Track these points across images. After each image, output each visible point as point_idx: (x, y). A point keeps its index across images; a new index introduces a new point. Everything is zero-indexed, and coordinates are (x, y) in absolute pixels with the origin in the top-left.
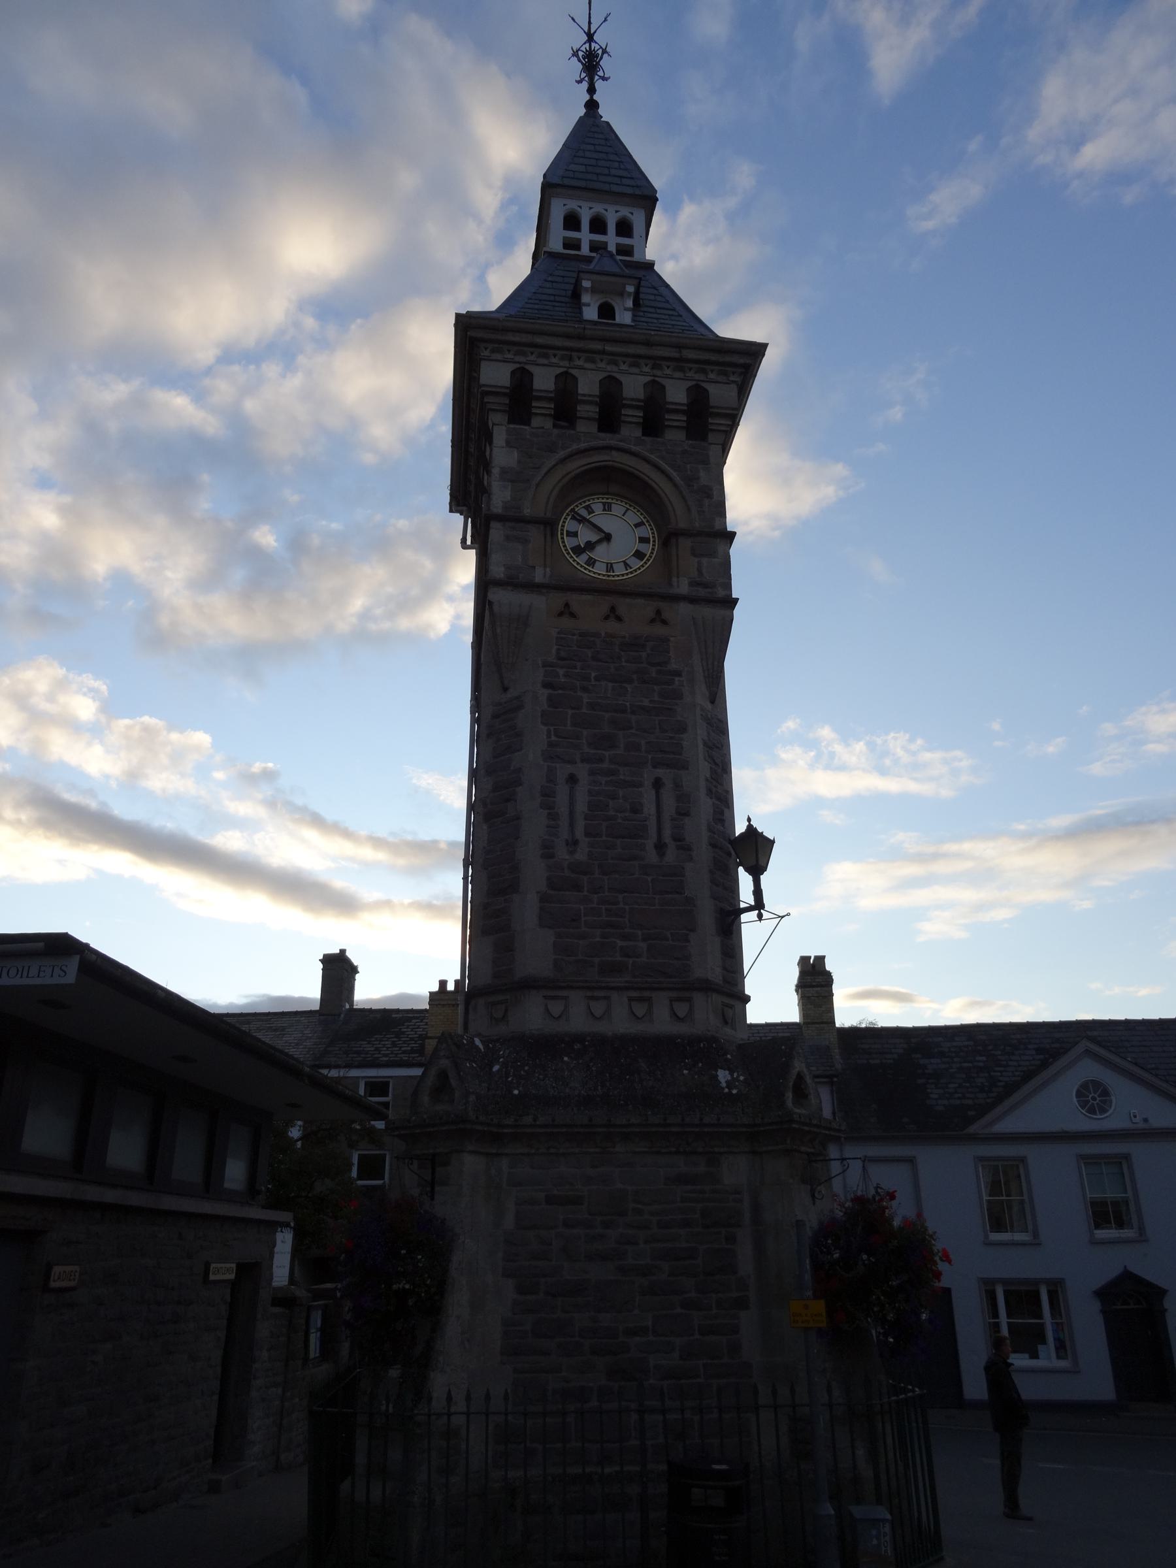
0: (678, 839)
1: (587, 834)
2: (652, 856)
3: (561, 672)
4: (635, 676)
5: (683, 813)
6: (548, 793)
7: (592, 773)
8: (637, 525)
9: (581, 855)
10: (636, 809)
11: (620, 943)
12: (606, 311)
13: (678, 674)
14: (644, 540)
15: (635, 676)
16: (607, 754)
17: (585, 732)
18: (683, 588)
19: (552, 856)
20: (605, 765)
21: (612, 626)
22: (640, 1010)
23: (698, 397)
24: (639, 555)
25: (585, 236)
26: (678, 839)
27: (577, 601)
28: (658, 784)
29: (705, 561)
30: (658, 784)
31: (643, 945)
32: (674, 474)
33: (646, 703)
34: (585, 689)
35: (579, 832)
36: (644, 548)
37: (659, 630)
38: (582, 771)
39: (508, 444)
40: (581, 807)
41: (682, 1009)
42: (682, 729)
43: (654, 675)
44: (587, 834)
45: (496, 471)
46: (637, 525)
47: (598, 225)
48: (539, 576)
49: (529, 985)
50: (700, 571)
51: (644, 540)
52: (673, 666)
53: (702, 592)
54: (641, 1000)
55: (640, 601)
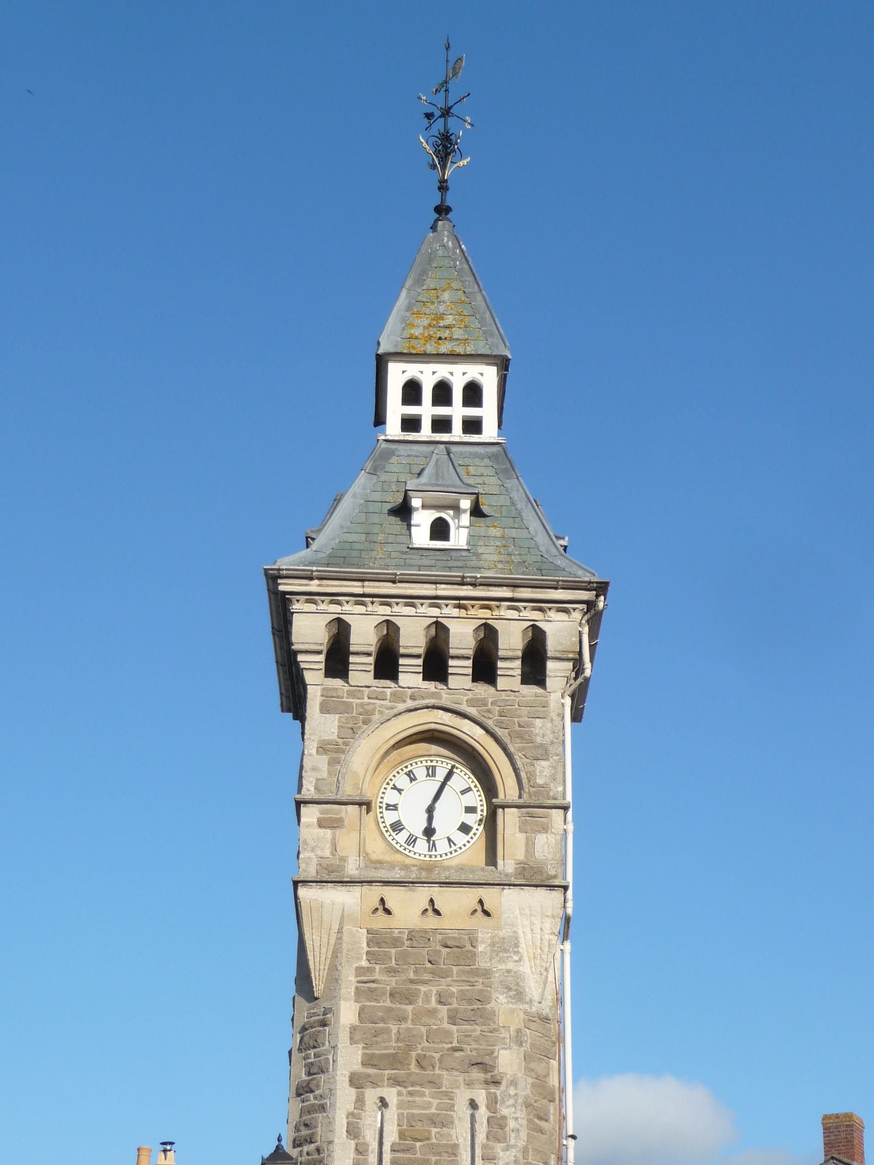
8: (463, 792)
12: (440, 530)
14: (470, 810)
24: (465, 828)
25: (427, 410)
27: (394, 897)
46: (463, 792)
48: (352, 869)
51: (470, 810)
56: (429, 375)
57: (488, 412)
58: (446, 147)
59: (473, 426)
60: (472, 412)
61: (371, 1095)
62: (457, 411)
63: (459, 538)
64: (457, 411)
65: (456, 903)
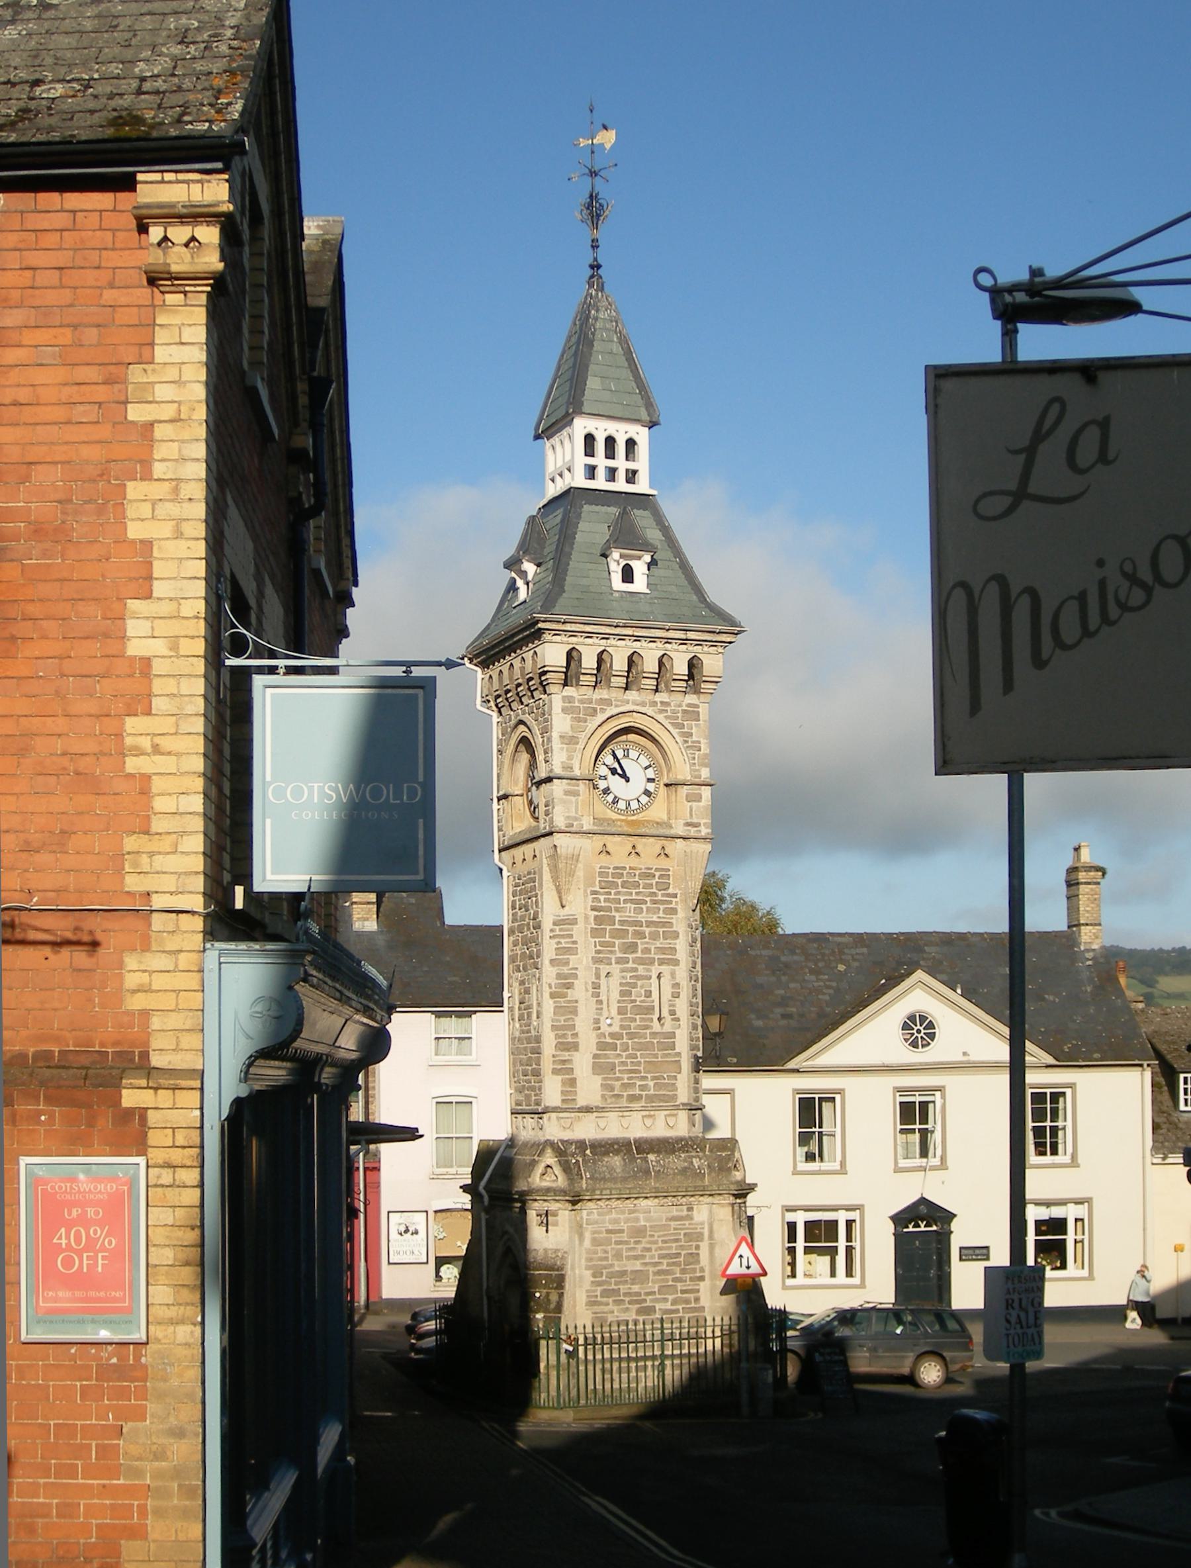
0: (672, 1013)
1: (619, 1013)
2: (656, 1027)
3: (602, 898)
4: (648, 899)
5: (676, 995)
6: (596, 986)
7: (622, 971)
8: (646, 768)
9: (616, 1028)
10: (649, 994)
11: (639, 1083)
13: (675, 896)
14: (650, 780)
15: (648, 899)
16: (630, 956)
17: (617, 942)
18: (680, 830)
19: (599, 1028)
20: (630, 965)
21: (633, 861)
22: (648, 1122)
23: (693, 665)
24: (647, 793)
25: (600, 461)
26: (672, 1013)
27: (612, 842)
28: (659, 977)
29: (694, 804)
30: (659, 977)
31: (651, 1084)
32: (675, 732)
33: (655, 919)
34: (617, 910)
35: (614, 1012)
36: (651, 787)
37: (663, 863)
38: (615, 969)
39: (564, 710)
40: (615, 995)
41: (671, 1121)
42: (676, 935)
43: (660, 898)
44: (619, 1013)
45: (555, 735)
46: (646, 768)
47: (610, 441)
49: (588, 1110)
50: (691, 815)
51: (650, 780)
52: (671, 891)
53: (692, 832)
54: (650, 1116)
55: (652, 840)
56: (601, 429)
57: (642, 463)
58: (594, 210)
59: (631, 476)
60: (631, 465)
61: (604, 968)
62: (621, 463)
63: (640, 584)
64: (621, 463)
65: (649, 847)
